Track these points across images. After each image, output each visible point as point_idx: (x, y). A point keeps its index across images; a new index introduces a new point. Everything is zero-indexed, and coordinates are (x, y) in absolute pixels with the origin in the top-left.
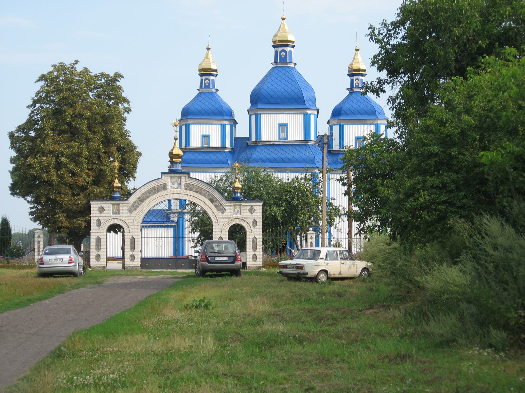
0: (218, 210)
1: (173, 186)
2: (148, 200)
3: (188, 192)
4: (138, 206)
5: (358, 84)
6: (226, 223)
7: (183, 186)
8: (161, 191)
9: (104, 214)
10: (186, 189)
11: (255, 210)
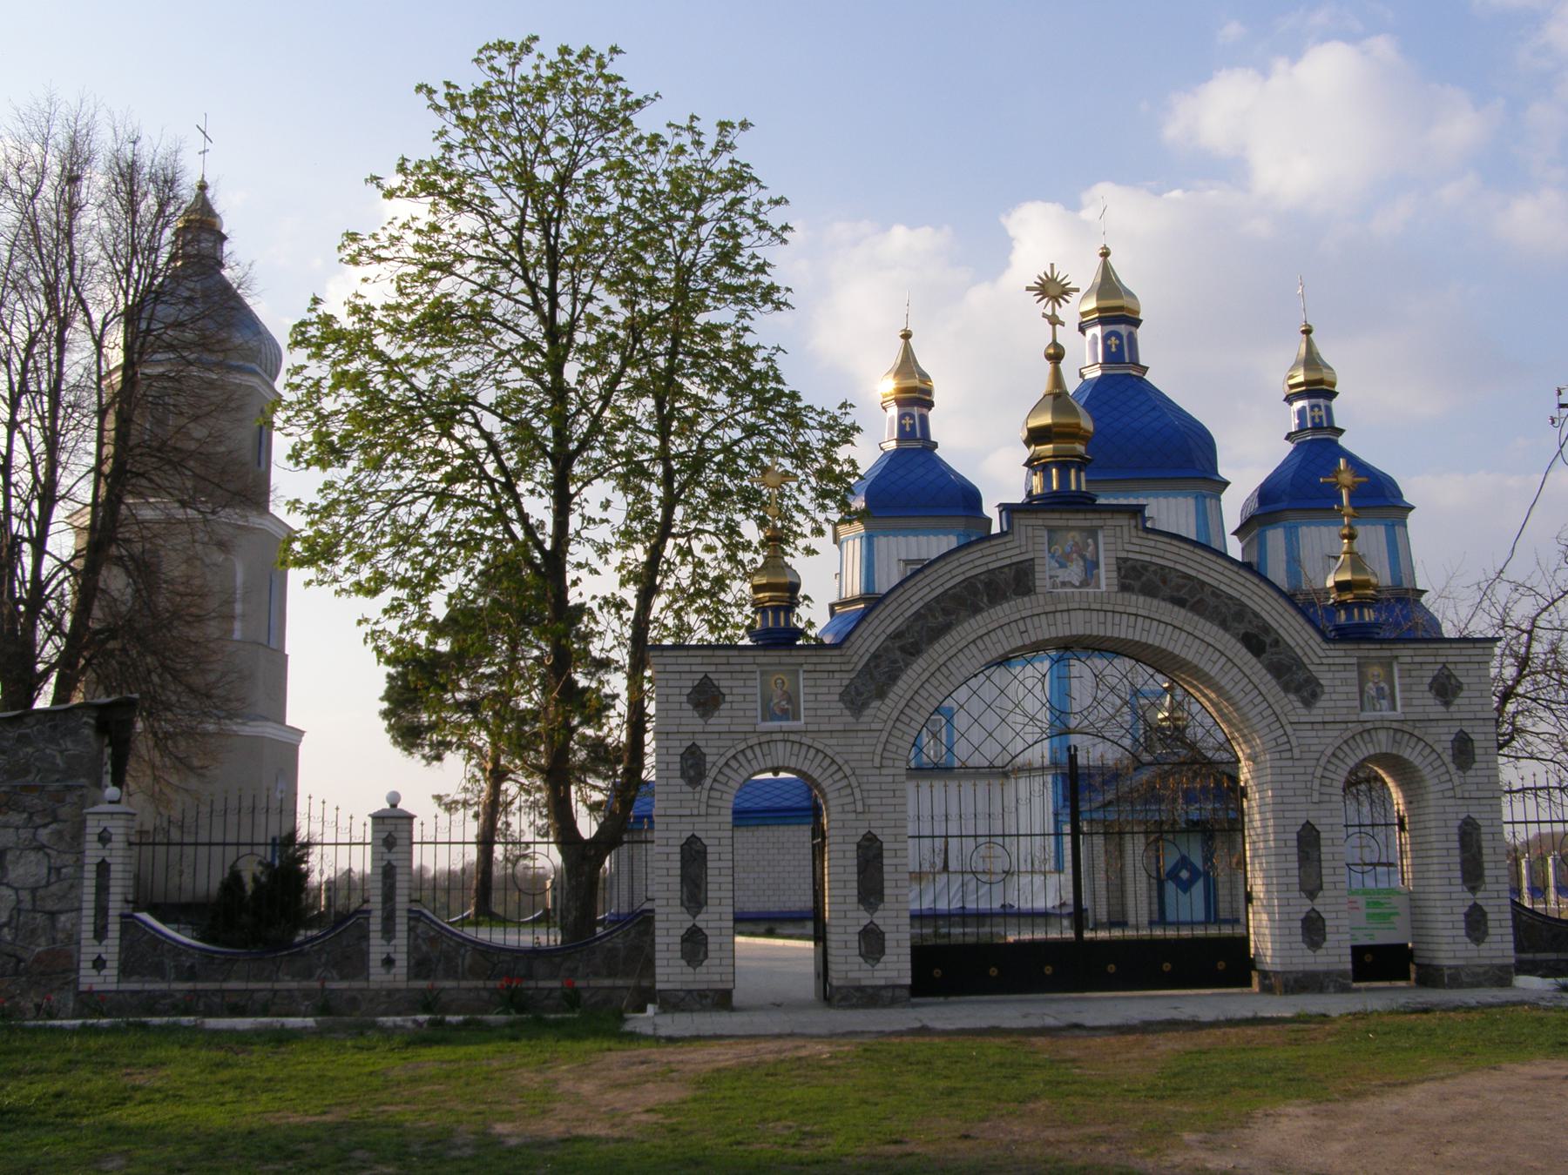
0: (1286, 688)
1: (1063, 575)
2: (938, 651)
3: (1139, 603)
4: (893, 678)
5: (1320, 417)
6: (1329, 751)
7: (1106, 577)
8: (1005, 598)
9: (719, 721)
10: (1124, 588)
11: (1459, 687)
